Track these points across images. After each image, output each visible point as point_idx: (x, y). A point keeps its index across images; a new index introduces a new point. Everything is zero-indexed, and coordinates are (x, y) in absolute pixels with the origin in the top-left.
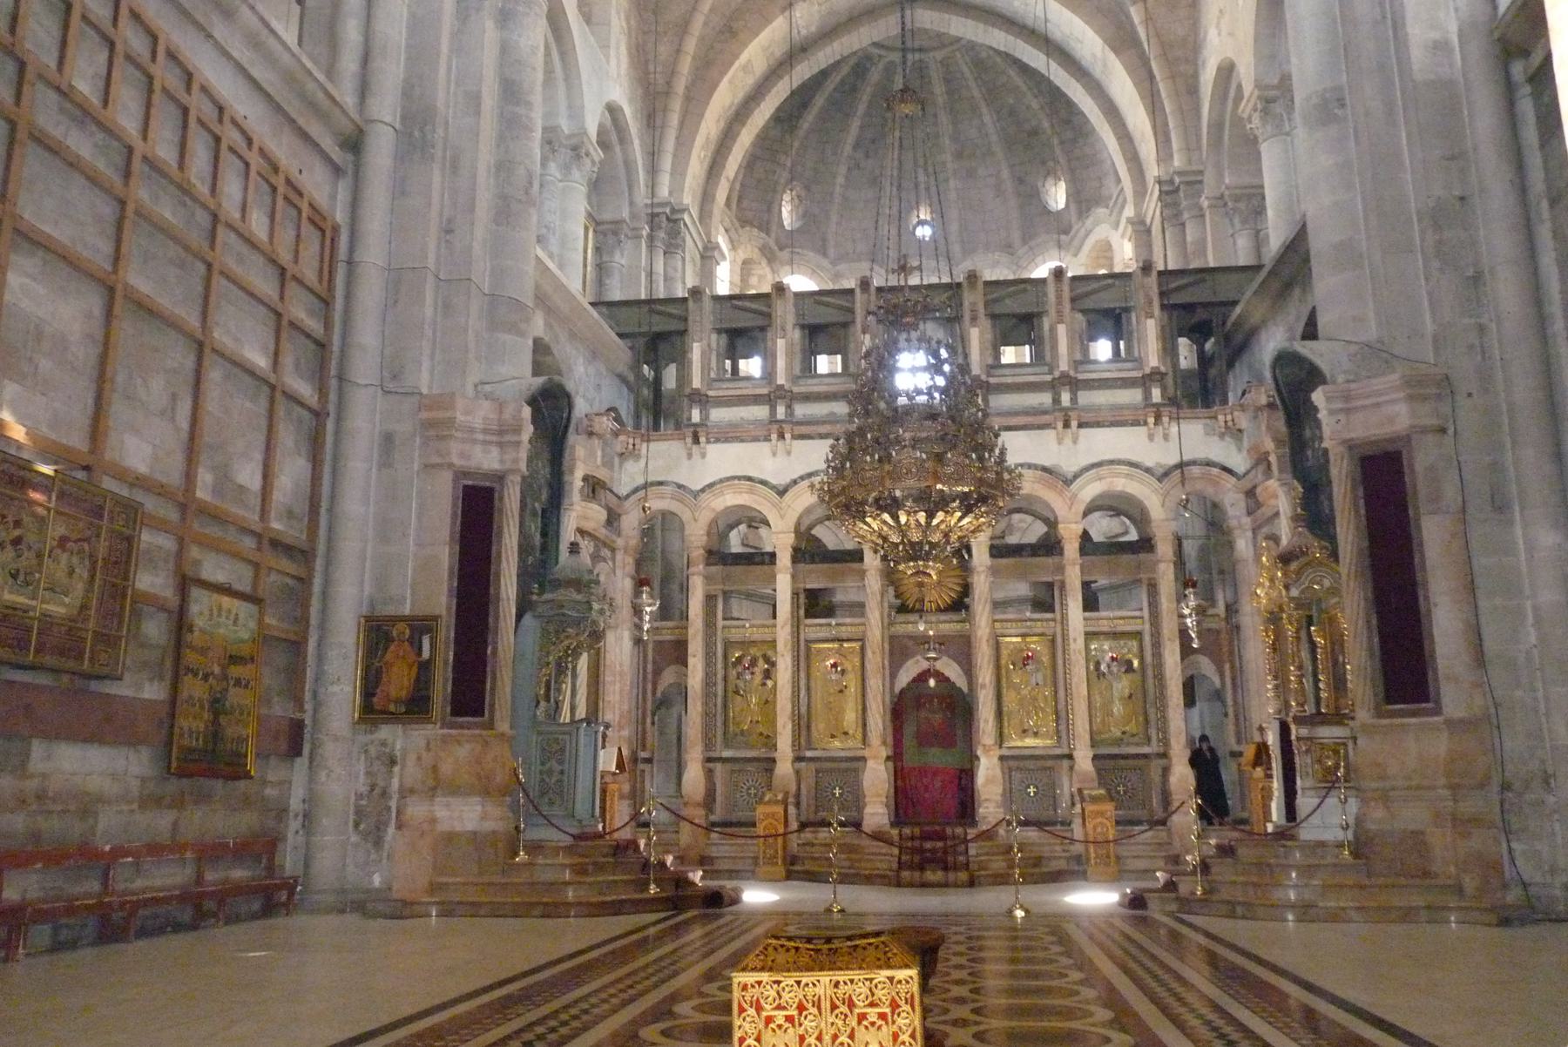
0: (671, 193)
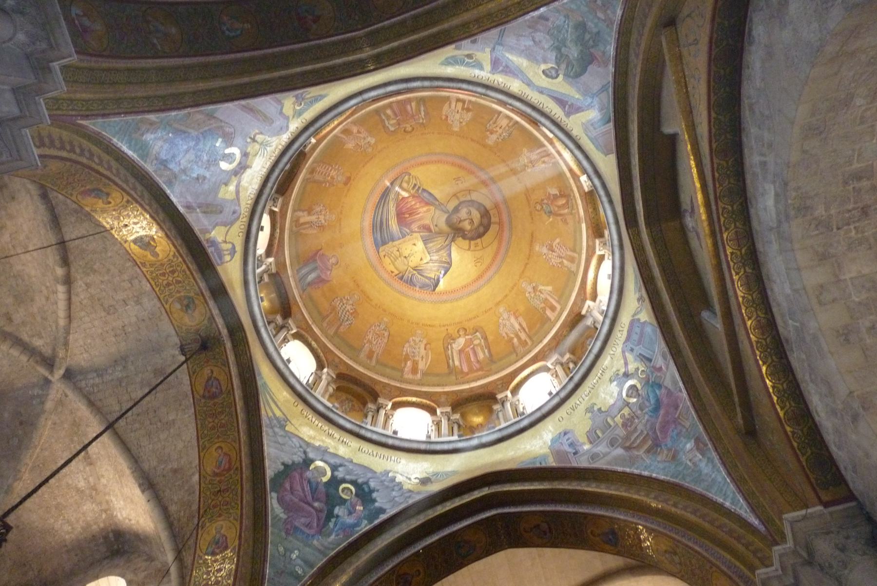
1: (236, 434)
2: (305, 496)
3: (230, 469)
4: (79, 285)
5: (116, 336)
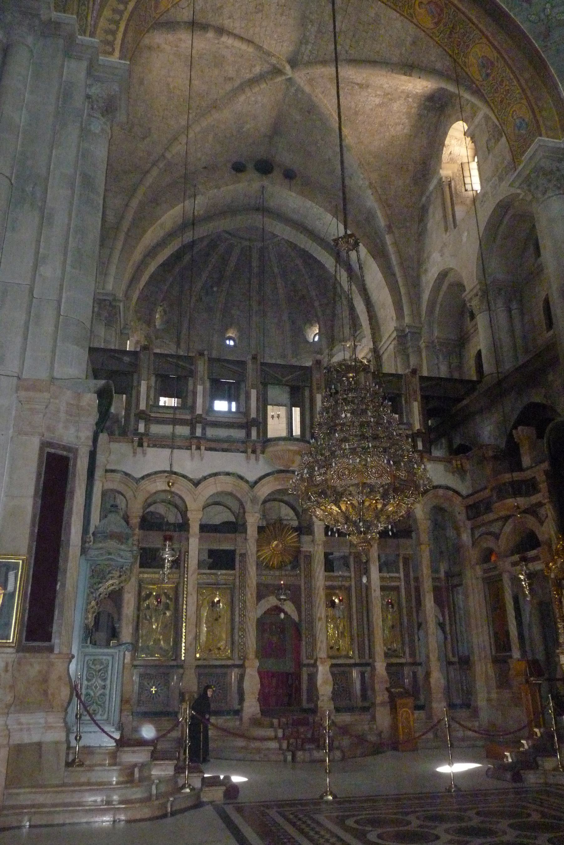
0: (113, 288)
3: (442, 10)
4: (227, 23)
5: (282, 15)
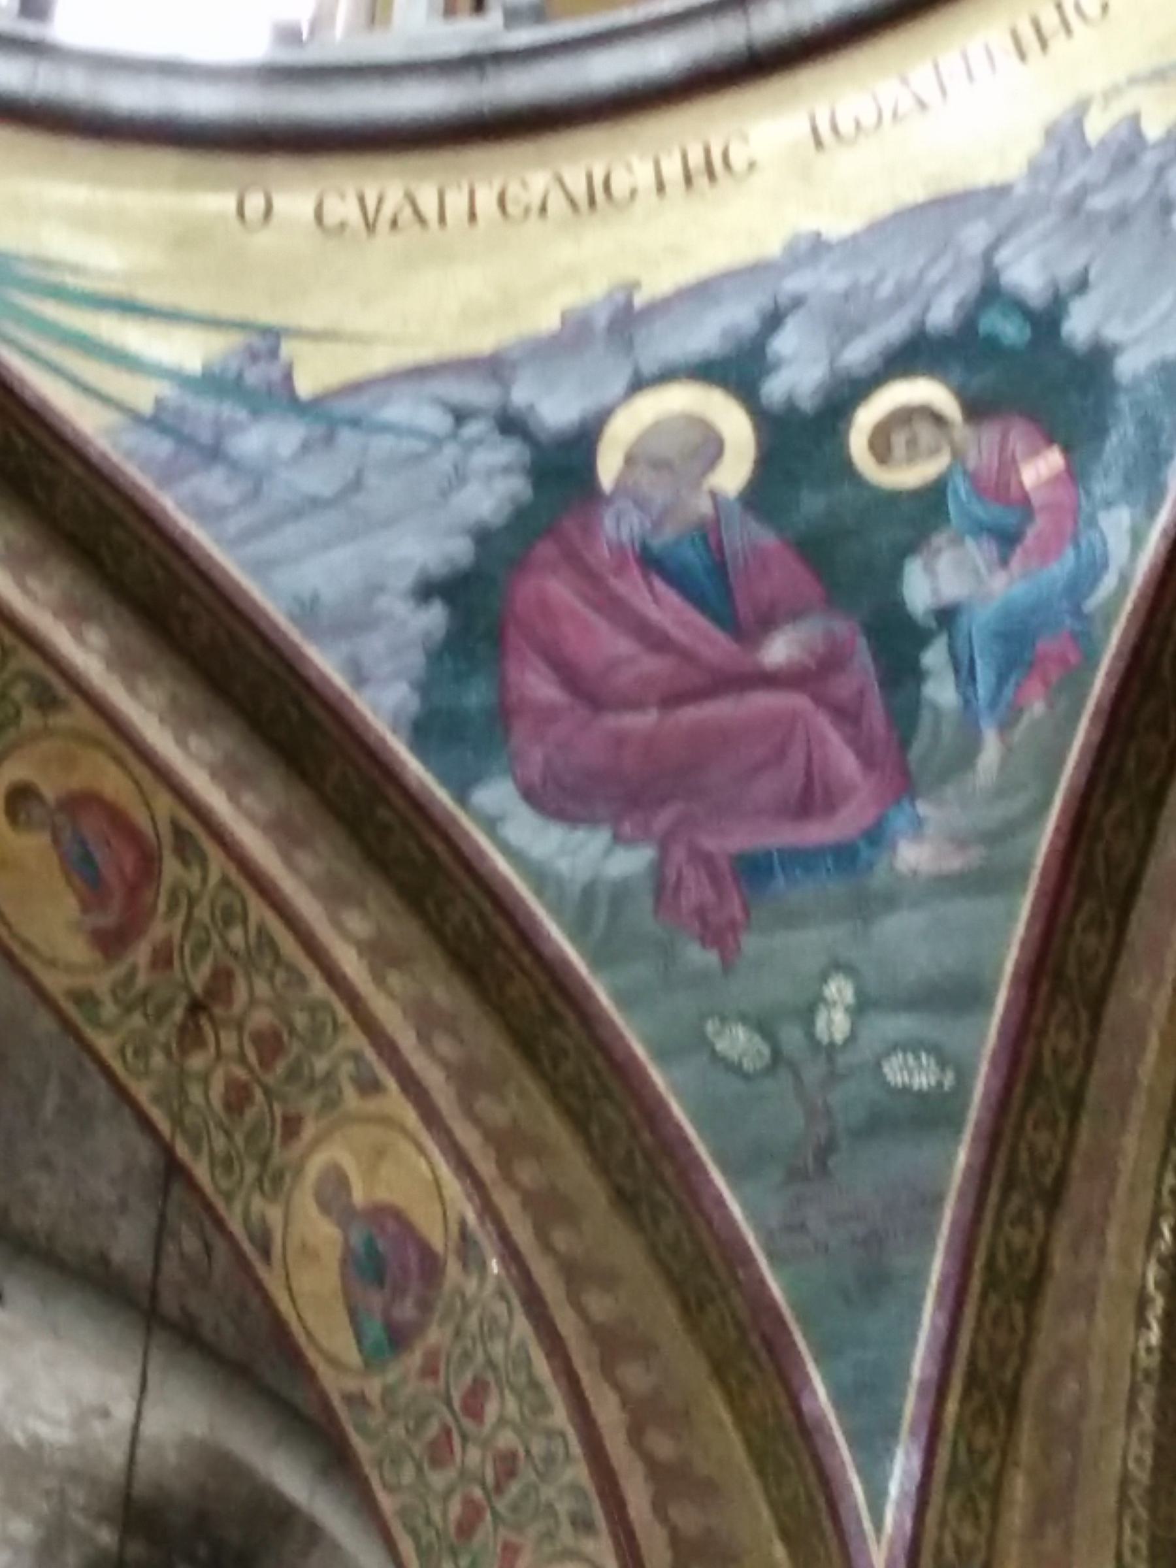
1: (30, 661)
2: (687, 656)
3: (149, 863)
